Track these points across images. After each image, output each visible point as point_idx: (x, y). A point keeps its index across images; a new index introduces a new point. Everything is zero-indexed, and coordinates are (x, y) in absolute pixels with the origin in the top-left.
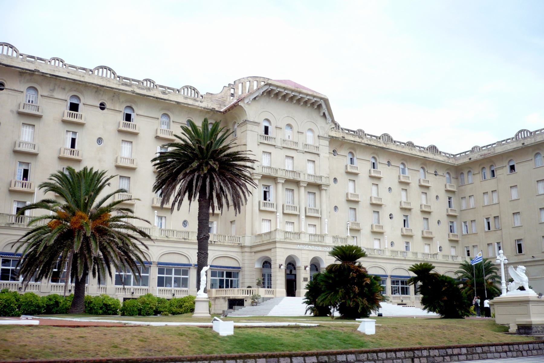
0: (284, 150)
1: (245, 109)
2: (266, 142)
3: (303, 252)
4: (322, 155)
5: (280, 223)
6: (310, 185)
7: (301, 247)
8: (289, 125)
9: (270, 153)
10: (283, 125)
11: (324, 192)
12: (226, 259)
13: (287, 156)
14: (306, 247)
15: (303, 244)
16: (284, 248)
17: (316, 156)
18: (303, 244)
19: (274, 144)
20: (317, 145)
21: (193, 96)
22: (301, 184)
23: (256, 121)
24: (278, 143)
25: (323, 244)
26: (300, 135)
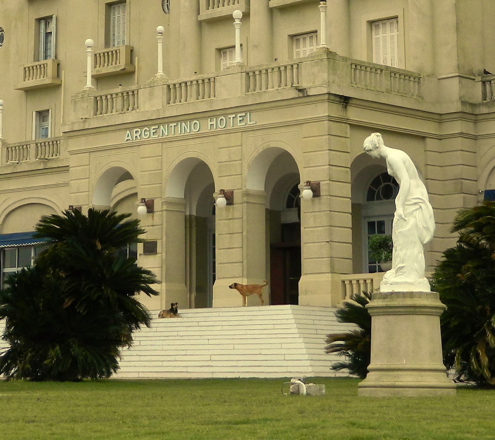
3: (147, 150)
7: (134, 135)
14: (148, 134)
16: (91, 151)
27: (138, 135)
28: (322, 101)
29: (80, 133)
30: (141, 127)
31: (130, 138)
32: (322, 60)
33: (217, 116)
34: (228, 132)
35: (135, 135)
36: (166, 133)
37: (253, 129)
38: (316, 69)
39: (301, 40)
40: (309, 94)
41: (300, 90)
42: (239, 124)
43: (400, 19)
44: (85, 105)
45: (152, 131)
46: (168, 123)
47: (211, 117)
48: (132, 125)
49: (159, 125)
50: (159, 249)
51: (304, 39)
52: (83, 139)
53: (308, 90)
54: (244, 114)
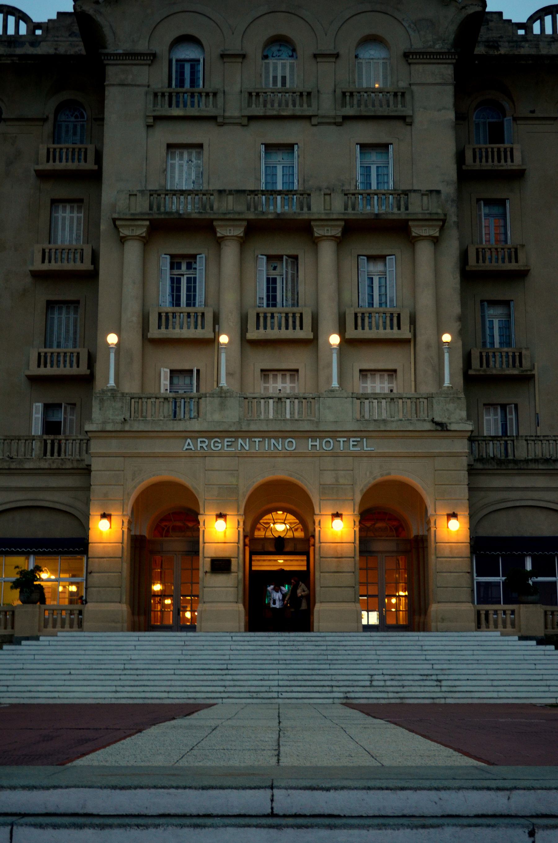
0: (255, 127)
1: (99, 19)
2: (176, 112)
4: (421, 119)
5: (229, 374)
6: (354, 230)
7: (201, 444)
8: (280, 42)
9: (200, 146)
10: (253, 47)
11: (424, 251)
12: (38, 517)
13: (270, 148)
15: (209, 434)
17: (399, 124)
18: (209, 434)
19: (211, 111)
20: (402, 84)
21: (11, 31)
22: (318, 232)
23: (142, 47)
24: (234, 109)
25: (307, 427)
26: (326, 67)
27: (204, 445)
28: (462, 437)
29: (113, 434)
30: (210, 438)
31: (192, 447)
32: (459, 398)
33: (322, 438)
34: (335, 455)
35: (199, 445)
36: (247, 448)
37: (369, 456)
38: (451, 406)
39: (271, 376)
40: (449, 428)
41: (437, 424)
42: (351, 449)
43: (399, 373)
44: (118, 405)
45: (226, 444)
46: (250, 438)
47: (314, 438)
48: (197, 435)
49: (237, 438)
50: (234, 567)
51: (275, 376)
52: (114, 442)
53: (448, 425)
54: (359, 439)
